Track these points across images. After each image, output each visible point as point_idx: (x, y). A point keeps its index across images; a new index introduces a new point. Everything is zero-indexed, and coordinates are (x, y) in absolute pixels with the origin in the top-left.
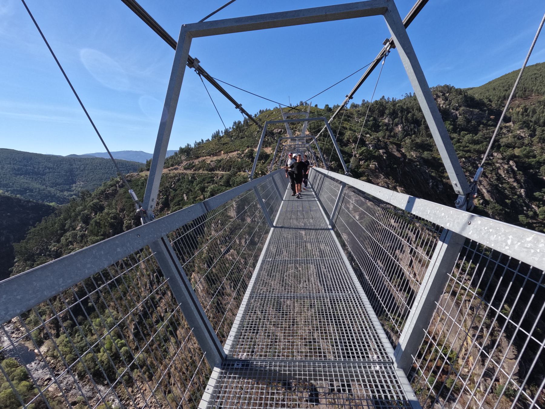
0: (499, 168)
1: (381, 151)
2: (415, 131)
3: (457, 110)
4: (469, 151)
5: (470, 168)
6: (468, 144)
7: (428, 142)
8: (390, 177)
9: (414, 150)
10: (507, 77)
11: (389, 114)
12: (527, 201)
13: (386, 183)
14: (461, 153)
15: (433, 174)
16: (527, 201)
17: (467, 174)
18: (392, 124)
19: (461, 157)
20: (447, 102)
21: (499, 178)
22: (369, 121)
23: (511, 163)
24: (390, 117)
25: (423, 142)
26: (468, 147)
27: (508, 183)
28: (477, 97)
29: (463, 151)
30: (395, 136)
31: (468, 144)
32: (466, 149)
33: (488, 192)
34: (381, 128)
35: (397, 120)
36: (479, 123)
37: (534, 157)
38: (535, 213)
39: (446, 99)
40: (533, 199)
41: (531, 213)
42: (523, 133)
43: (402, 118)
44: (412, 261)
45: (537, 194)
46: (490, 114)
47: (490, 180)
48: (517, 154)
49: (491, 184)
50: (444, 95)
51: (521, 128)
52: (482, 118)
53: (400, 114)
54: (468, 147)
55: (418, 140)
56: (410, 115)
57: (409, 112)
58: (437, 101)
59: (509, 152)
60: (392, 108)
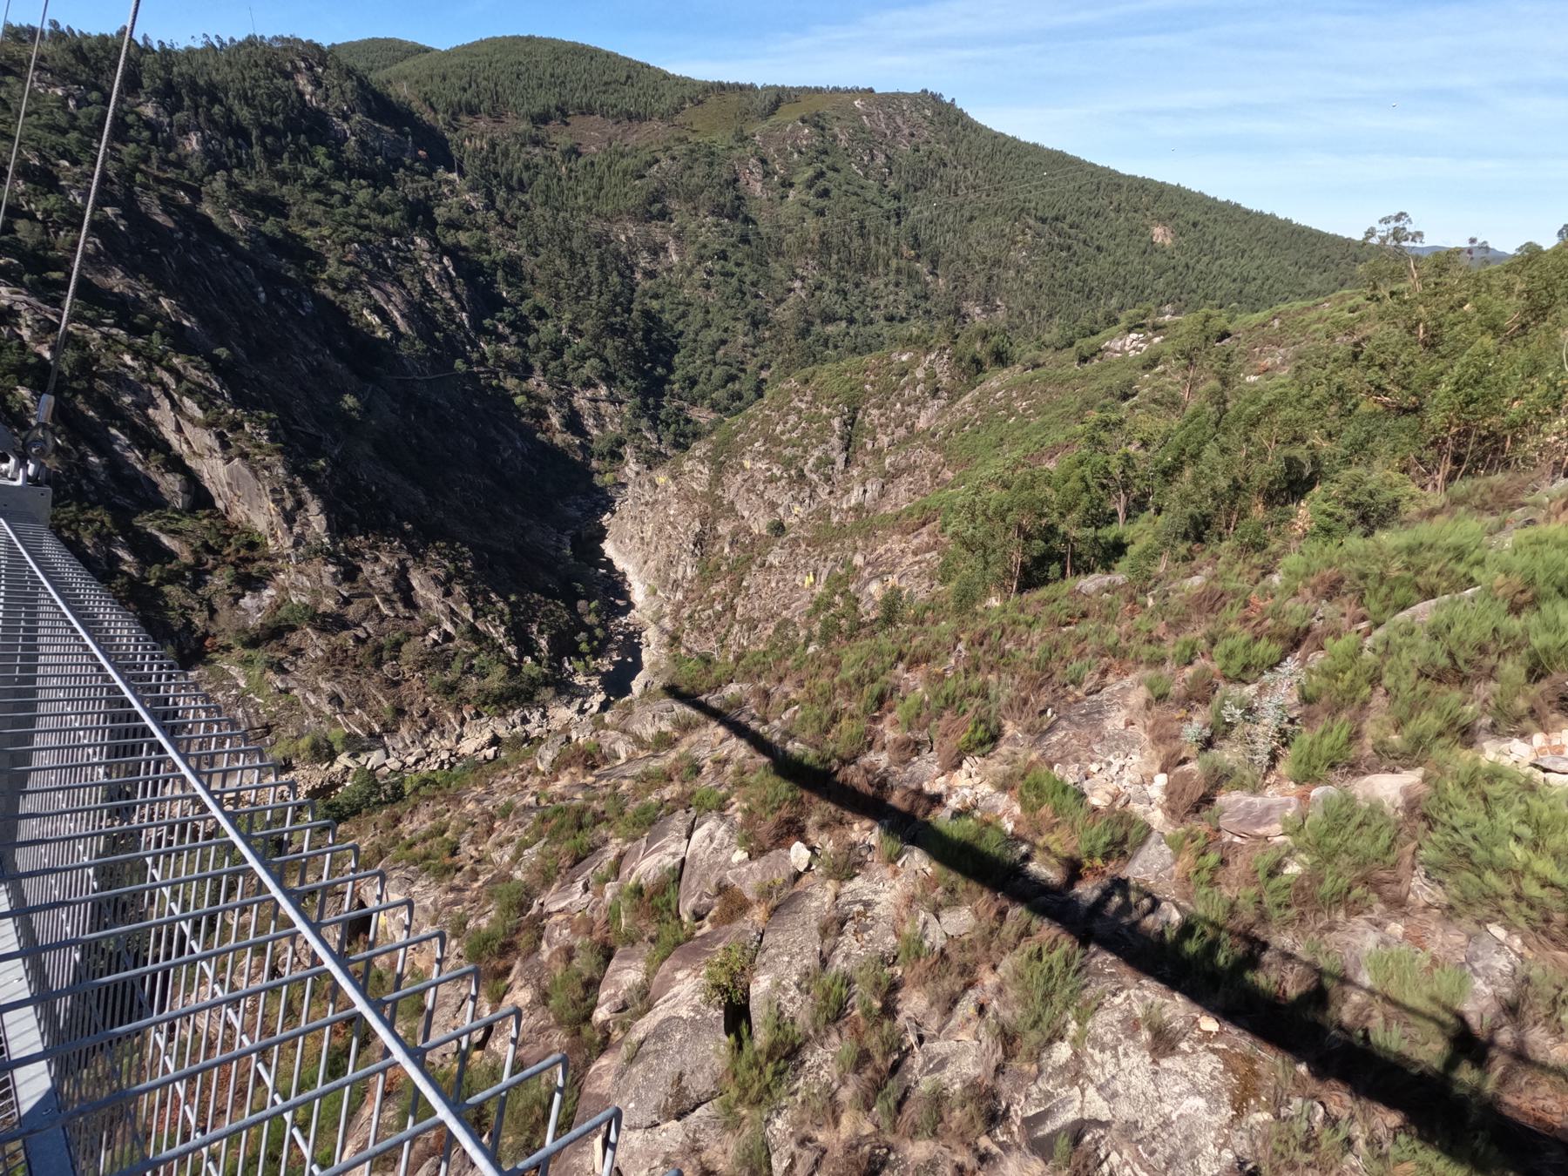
0: (425, 270)
1: (109, 210)
2: (239, 159)
3: (346, 118)
4: (367, 228)
5: (370, 266)
6: (366, 211)
7: (277, 193)
8: (142, 276)
9: (241, 211)
10: (475, 51)
11: (156, 92)
12: (472, 334)
13: (130, 287)
14: (351, 231)
15: (291, 274)
16: (472, 334)
17: (364, 278)
18: (171, 125)
19: (350, 240)
20: (319, 92)
21: (427, 290)
22: (90, 104)
23: (446, 260)
24: (162, 104)
25: (262, 190)
26: (366, 217)
27: (442, 300)
28: (402, 91)
29: (356, 225)
30: (180, 164)
31: (366, 211)
32: (363, 221)
33: (403, 316)
34: (132, 132)
35: (180, 117)
36: (397, 164)
37: (489, 253)
38: (483, 355)
39: (317, 82)
40: (481, 330)
41: (475, 356)
42: (475, 200)
43: (197, 114)
44: (178, 423)
45: (487, 322)
46: (418, 145)
47: (409, 293)
48: (464, 243)
49: (409, 302)
50: (310, 68)
51: (473, 189)
52: (404, 151)
53: (187, 102)
54: (366, 217)
55: (251, 186)
56: (217, 109)
57: (214, 99)
58: (296, 84)
59: (449, 238)
60: (162, 73)
